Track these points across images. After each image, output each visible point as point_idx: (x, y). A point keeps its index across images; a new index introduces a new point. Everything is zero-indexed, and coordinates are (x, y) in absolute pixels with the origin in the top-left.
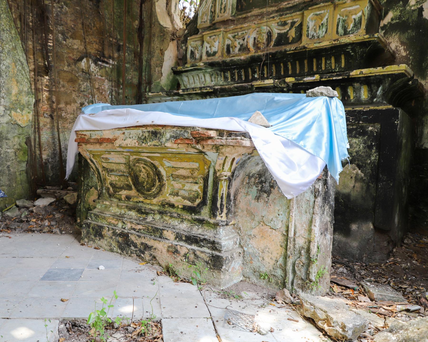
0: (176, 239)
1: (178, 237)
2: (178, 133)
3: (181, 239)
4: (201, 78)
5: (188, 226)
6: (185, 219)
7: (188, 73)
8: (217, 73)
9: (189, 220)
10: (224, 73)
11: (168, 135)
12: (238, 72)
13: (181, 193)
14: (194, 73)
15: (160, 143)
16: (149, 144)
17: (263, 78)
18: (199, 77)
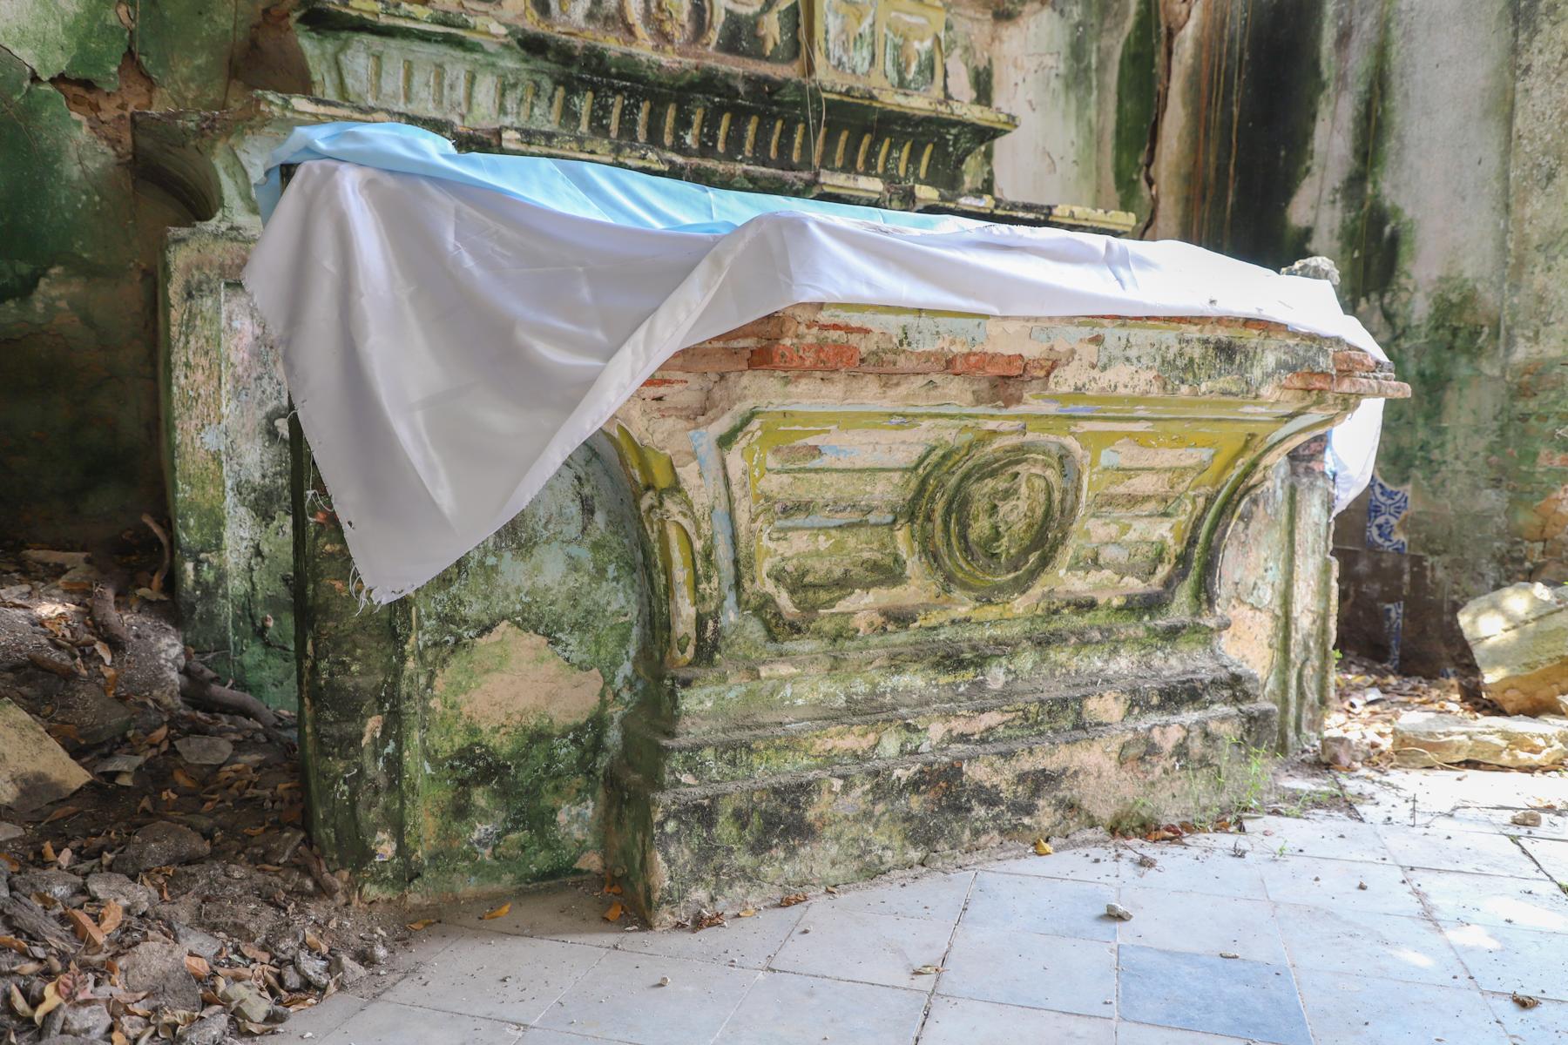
0: (1129, 712)
1: (1137, 702)
2: (1301, 353)
3: (1149, 708)
4: (452, 87)
5: (1134, 659)
6: (1124, 641)
7: (394, 43)
8: (537, 85)
9: (1136, 640)
10: (571, 91)
11: (1270, 360)
12: (624, 109)
13: (1108, 554)
14: (425, 52)
15: (1243, 385)
16: (1203, 387)
17: (849, 167)
18: (440, 77)
